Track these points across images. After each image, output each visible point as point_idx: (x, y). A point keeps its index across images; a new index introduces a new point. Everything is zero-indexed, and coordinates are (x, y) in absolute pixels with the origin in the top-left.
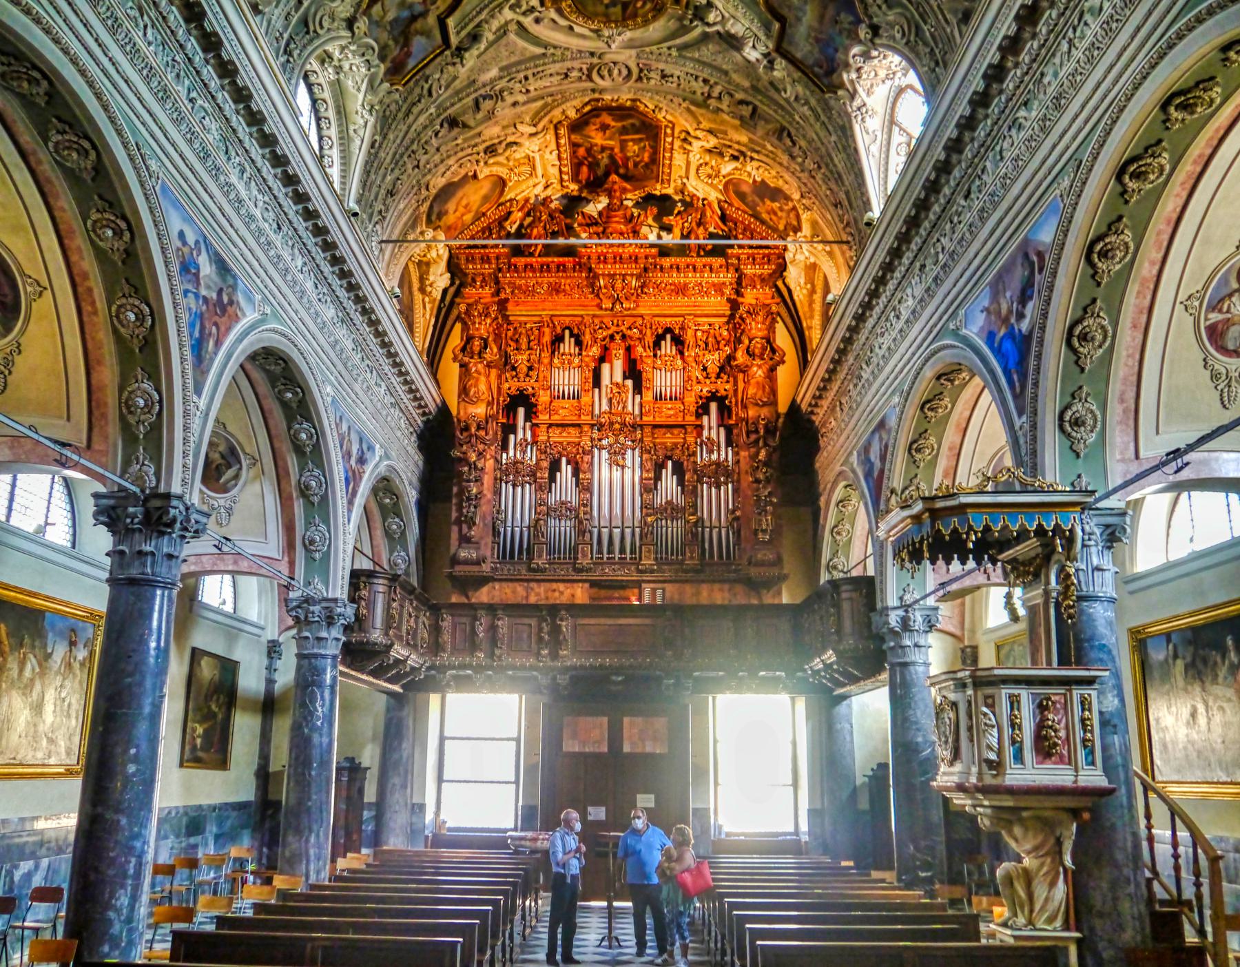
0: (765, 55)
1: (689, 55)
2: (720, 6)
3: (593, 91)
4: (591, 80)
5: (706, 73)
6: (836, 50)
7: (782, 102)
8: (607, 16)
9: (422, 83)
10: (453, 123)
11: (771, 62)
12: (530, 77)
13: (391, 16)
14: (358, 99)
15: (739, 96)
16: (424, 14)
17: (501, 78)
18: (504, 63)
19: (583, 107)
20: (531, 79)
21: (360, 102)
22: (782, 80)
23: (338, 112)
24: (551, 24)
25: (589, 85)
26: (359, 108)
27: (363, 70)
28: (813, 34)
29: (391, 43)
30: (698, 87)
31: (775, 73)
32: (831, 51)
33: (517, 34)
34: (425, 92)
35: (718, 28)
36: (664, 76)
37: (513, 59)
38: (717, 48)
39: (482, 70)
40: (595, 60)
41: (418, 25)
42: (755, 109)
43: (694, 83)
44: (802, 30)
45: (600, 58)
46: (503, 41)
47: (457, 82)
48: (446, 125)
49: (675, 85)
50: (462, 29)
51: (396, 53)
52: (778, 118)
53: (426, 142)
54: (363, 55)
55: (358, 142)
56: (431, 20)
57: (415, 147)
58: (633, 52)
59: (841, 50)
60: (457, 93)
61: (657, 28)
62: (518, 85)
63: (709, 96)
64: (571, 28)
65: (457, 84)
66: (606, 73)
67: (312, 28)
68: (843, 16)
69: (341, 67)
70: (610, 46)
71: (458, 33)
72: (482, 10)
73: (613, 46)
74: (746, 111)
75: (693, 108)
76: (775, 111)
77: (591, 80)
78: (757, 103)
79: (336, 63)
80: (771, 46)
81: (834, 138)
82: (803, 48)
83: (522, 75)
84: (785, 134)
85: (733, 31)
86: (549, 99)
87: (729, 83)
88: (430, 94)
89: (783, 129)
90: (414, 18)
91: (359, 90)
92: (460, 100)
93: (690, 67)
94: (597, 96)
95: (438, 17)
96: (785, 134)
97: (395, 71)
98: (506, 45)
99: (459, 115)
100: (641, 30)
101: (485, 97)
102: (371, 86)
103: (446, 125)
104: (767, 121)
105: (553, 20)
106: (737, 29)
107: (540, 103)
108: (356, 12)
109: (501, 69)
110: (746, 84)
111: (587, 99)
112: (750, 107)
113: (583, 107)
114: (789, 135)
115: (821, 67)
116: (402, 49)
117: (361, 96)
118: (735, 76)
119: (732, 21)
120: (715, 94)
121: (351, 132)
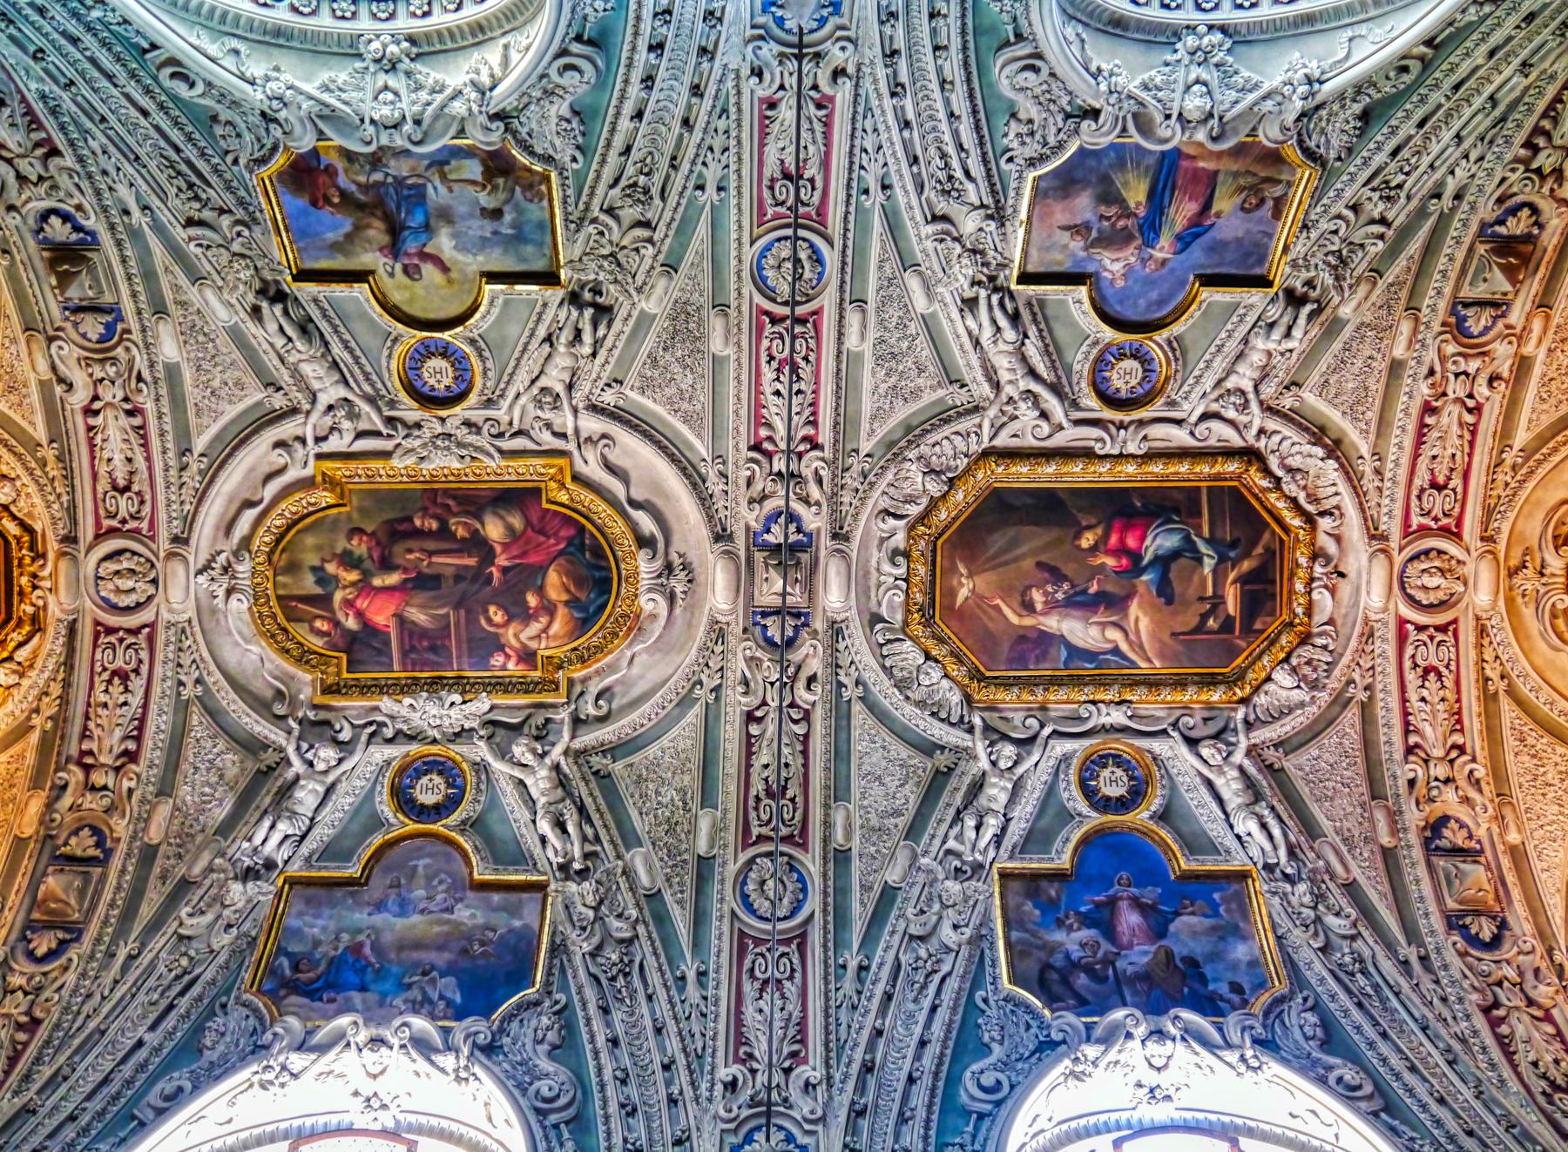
0: (270, 865)
1: (195, 719)
2: (347, 766)
3: (70, 539)
4: (99, 537)
5: (152, 752)
6: (363, 988)
7: (146, 911)
8: (293, 568)
9: (240, 214)
10: (68, 258)
11: (249, 874)
12: (137, 421)
13: (437, 193)
14: (305, 81)
15: (121, 827)
16: (394, 249)
17: (152, 365)
18: (188, 374)
19: (14, 518)
20: (124, 421)
21: (297, 83)
22: (219, 901)
23: (278, 32)
24: (267, 469)
25: (87, 531)
26: (287, 77)
27: (386, 111)
28: (361, 938)
29: (377, 176)
30: (109, 742)
31: (236, 887)
32: (352, 978)
33: (259, 404)
34: (207, 215)
35: (298, 766)
36: (123, 676)
37: (192, 393)
38: (232, 772)
39: (192, 332)
40: (164, 545)
41: (377, 232)
42: (103, 861)
43: (118, 733)
44: (360, 917)
45: (171, 555)
46: (250, 380)
47: (183, 280)
48: (74, 237)
49: (103, 698)
50: (323, 311)
51: (342, 180)
52: (101, 909)
53: (55, 187)
54: (418, 122)
55: (213, 50)
56: (370, 258)
57: (69, 161)
58: (191, 613)
59: (372, 997)
60: (149, 276)
61: (253, 656)
62: (120, 395)
63: (87, 769)
64: (249, 504)
65: (171, 279)
66: (125, 565)
67: (576, 48)
68: (450, 981)
69: (393, 68)
70: (200, 572)
71: (316, 301)
72: (351, 352)
73: (201, 579)
74: (82, 845)
75: (34, 737)
76: (112, 905)
77: (99, 537)
78: (116, 863)
79: (406, 64)
80: (295, 869)
81: (152, 1039)
82: (320, 928)
83: (149, 406)
84: (61, 935)
85: (299, 794)
86: (50, 454)
87: (143, 801)
88: (190, 223)
89: (74, 932)
90: (395, 231)
91: (326, 88)
92: (129, 278)
93: (159, 723)
94: (53, 546)
95: (372, 272)
96: (61, 935)
97: (306, 175)
98: (239, 384)
99: (92, 271)
100: (249, 630)
101: (110, 328)
102: (329, 115)
103: (74, 237)
104: (82, 893)
105: (281, 471)
106: (306, 797)
107: (40, 433)
108: (515, 133)
109: (173, 372)
110: (155, 834)
111: (38, 527)
112: (97, 852)
113: (14, 518)
114: (63, 945)
115: (296, 968)
116: (343, 194)
117: (309, 88)
118: (164, 810)
119: (321, 789)
120: (98, 778)
121: (235, 43)
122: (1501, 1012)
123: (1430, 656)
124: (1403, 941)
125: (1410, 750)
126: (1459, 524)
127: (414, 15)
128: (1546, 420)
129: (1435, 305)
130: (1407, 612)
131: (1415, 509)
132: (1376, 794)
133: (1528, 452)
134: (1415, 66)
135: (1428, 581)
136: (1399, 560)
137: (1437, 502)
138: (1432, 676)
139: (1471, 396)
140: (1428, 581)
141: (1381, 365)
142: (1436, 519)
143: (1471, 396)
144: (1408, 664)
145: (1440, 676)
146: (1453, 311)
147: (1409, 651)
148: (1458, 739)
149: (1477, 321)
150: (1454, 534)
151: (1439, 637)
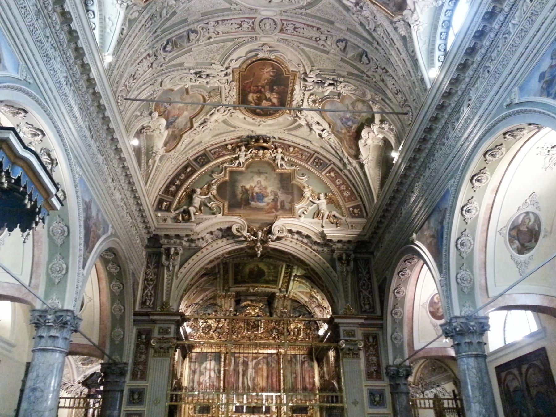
122: (148, 58)
123: (245, 25)
124: (162, 29)
125: (217, 22)
126: (283, 33)
127: (439, 57)
128: (310, 55)
129: (348, 36)
130: (258, 20)
131: (288, 22)
132: (203, 14)
133: (303, 50)
134: (413, 54)
135: (268, 24)
136: (274, 18)
137: (291, 28)
138: (238, 26)
139: (320, 39)
140: (268, 24)
141: (333, 19)
142: (285, 28)
143: (320, 39)
144: (242, 20)
145: (239, 28)
146: (345, 40)
147: (246, 20)
148: (221, 33)
149: (342, 45)
150: (281, 31)
151: (250, 28)
